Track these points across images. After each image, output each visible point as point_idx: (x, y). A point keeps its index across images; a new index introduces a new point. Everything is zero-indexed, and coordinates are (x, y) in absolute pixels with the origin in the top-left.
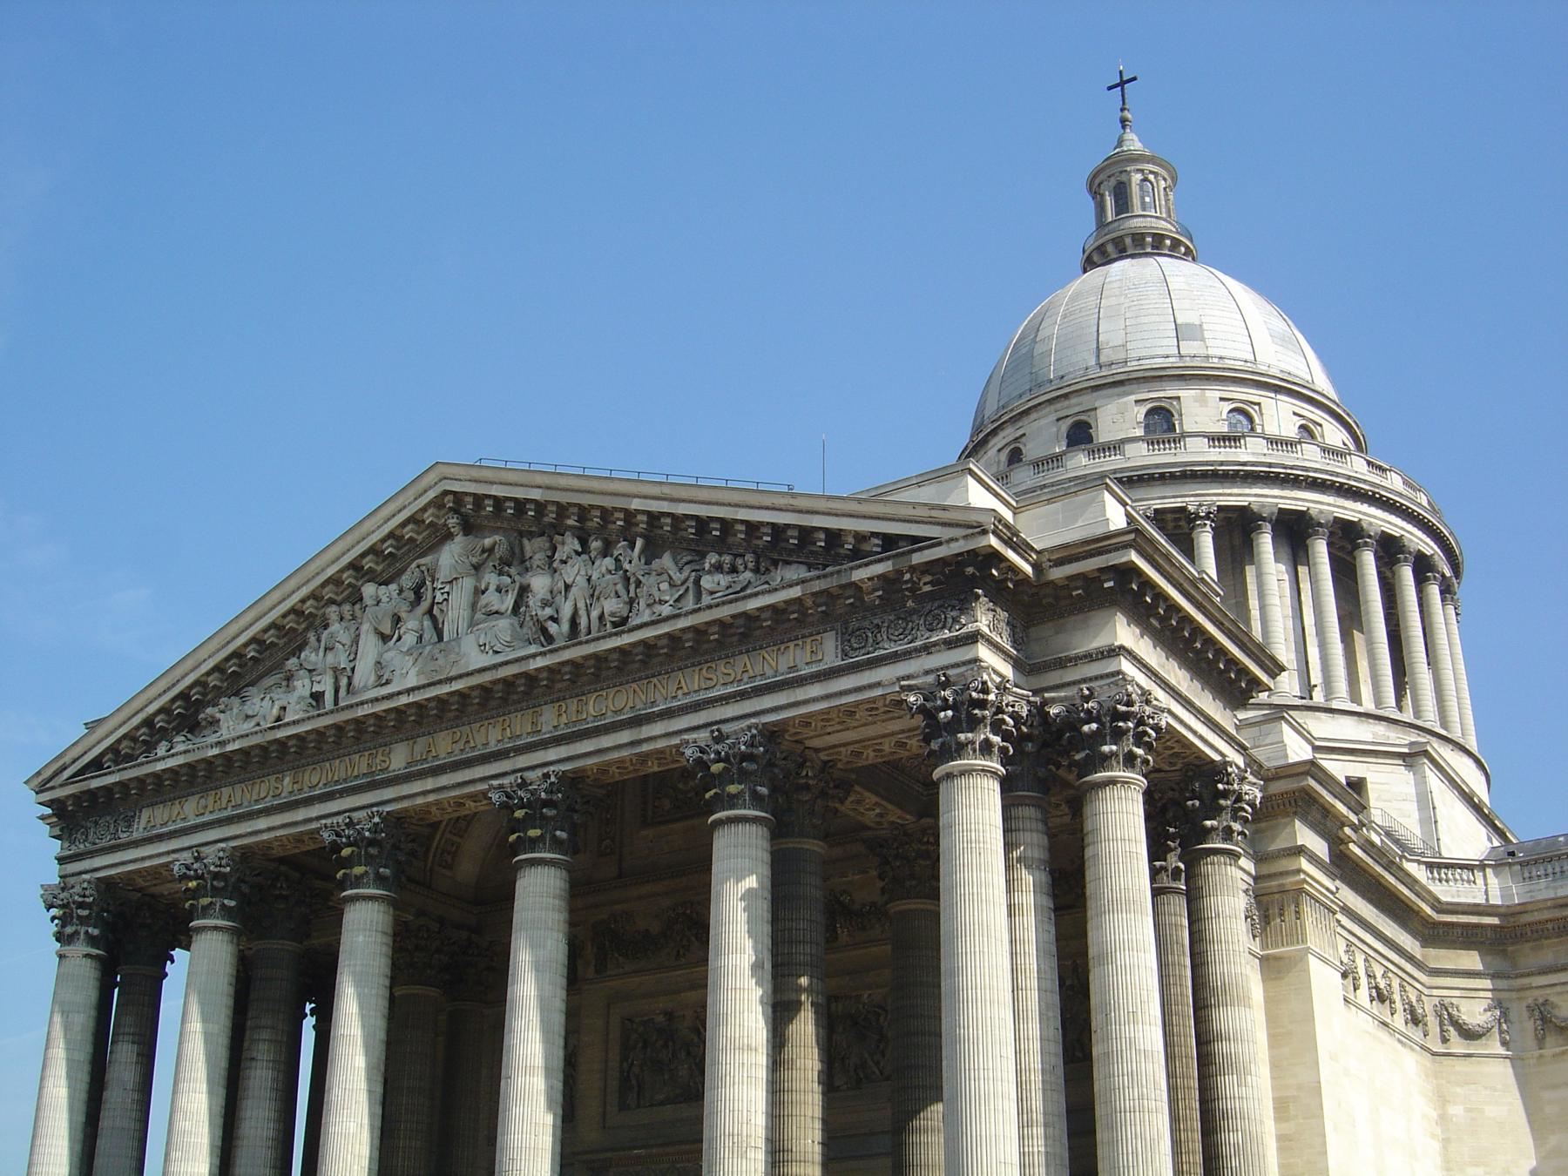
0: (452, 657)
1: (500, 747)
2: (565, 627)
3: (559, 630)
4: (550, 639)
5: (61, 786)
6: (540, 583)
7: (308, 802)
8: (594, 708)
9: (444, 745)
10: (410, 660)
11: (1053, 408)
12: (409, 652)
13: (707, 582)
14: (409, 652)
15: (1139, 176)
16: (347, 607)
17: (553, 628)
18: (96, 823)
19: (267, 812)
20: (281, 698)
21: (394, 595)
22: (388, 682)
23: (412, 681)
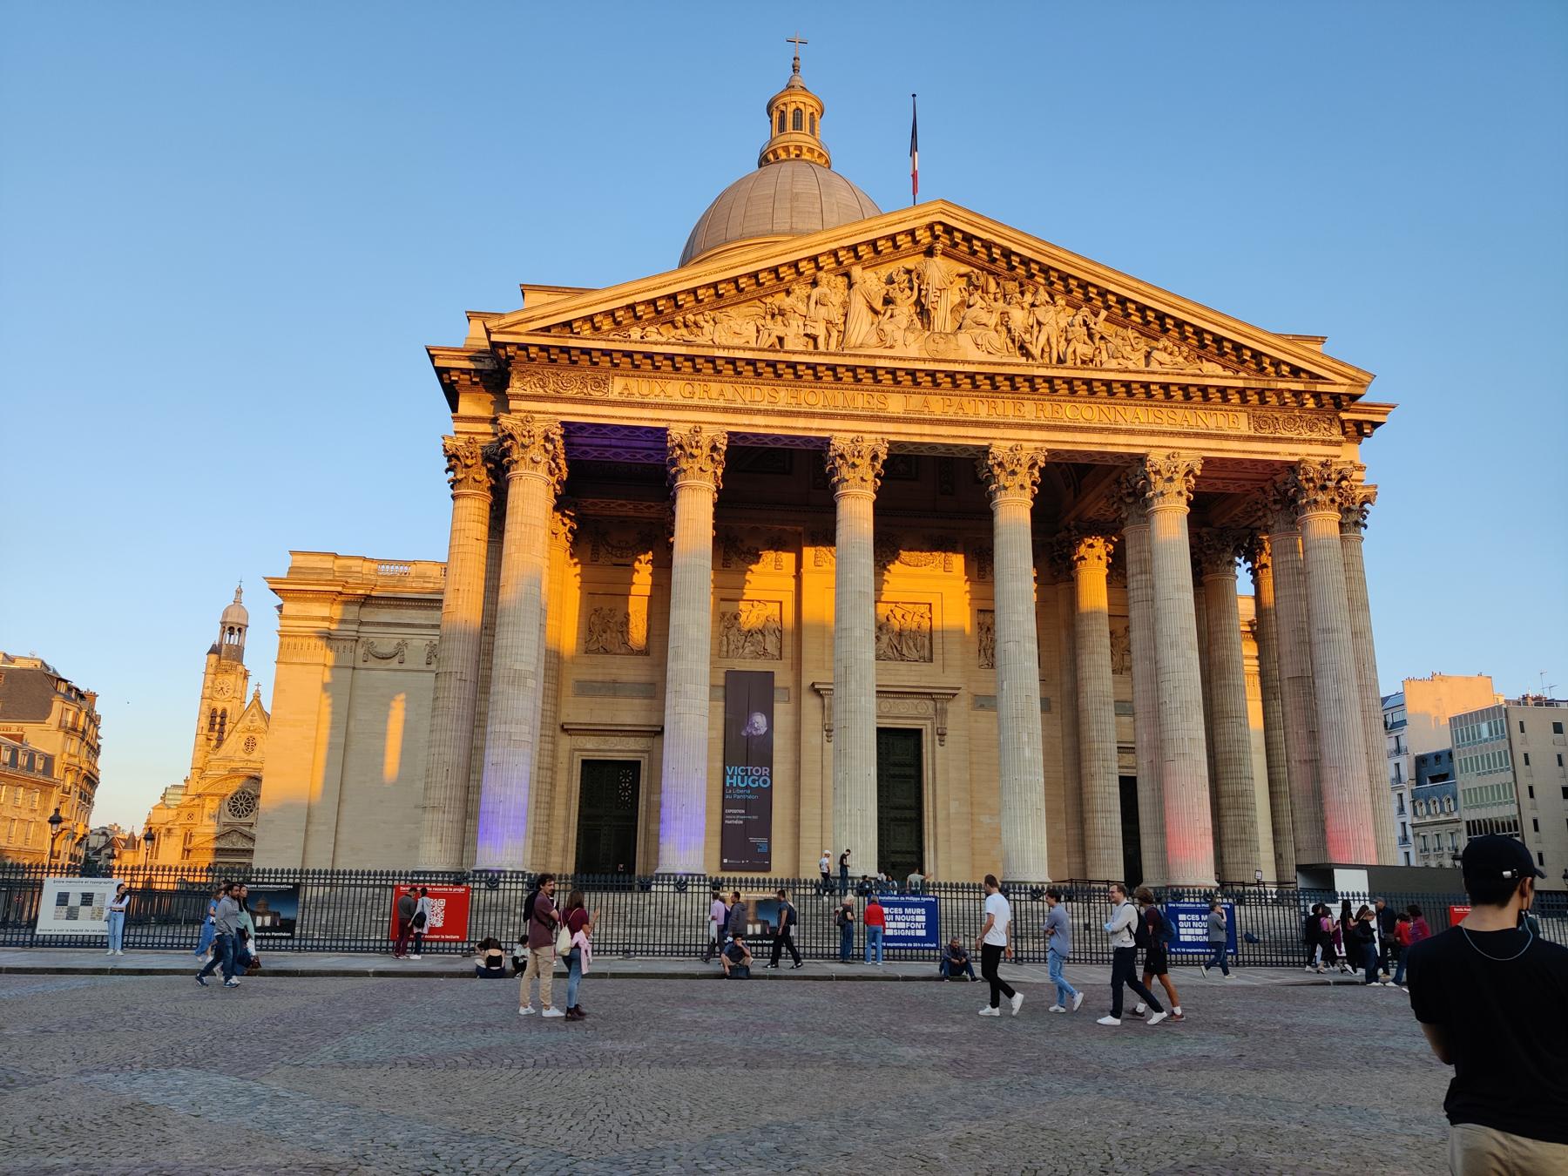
0: (952, 346)
3: (1036, 352)
4: (1027, 354)
5: (531, 333)
6: (1019, 318)
7: (812, 415)
8: (1070, 412)
9: (938, 405)
10: (911, 337)
13: (1155, 354)
15: (811, 110)
19: (766, 413)
23: (913, 352)
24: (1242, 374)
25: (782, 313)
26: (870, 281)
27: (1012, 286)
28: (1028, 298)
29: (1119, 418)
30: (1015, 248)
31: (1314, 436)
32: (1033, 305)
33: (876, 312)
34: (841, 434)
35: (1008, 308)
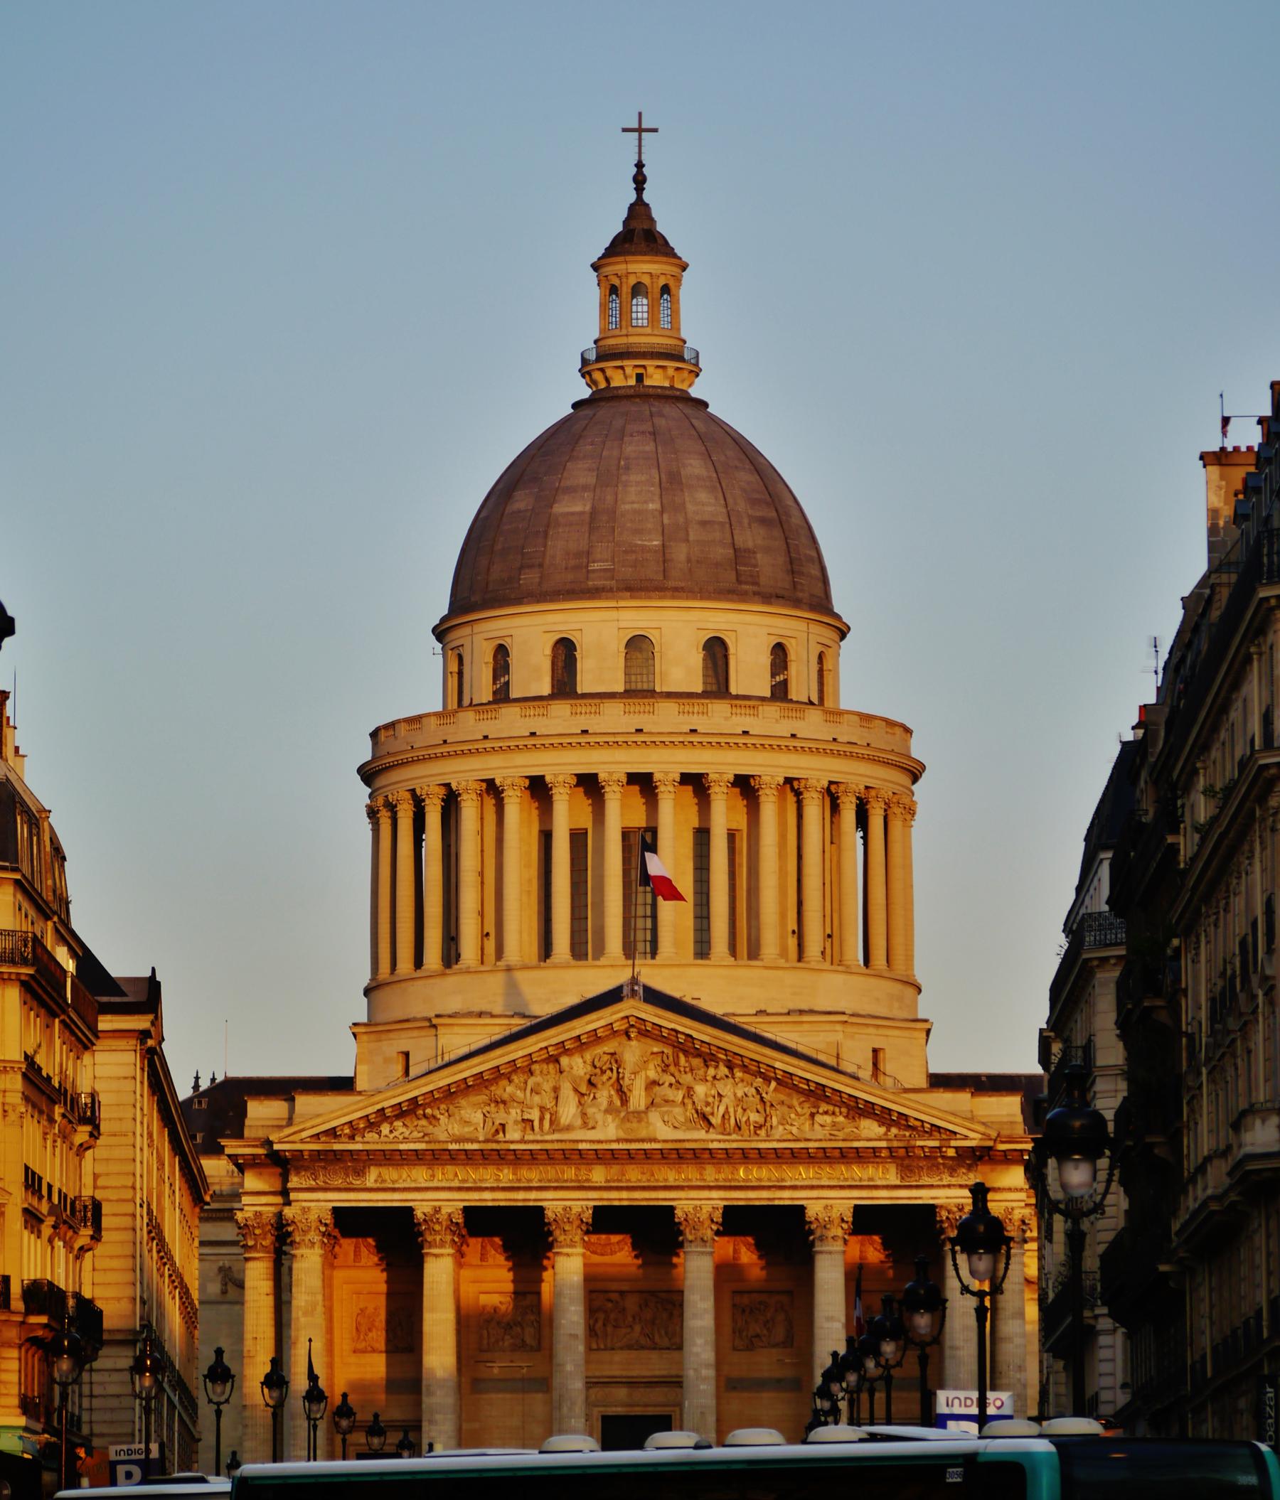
1: (677, 1184)
2: (719, 1120)
3: (716, 1120)
5: (302, 1141)
6: (700, 1090)
9: (634, 1174)
10: (610, 1118)
11: (613, 614)
12: (607, 1111)
13: (818, 1118)
14: (607, 1111)
16: (545, 1066)
17: (713, 1121)
18: (324, 1168)
19: (492, 1189)
20: (500, 1117)
21: (581, 1065)
22: (593, 1128)
24: (894, 1131)
25: (504, 1102)
26: (578, 1065)
27: (696, 1062)
28: (711, 1071)
29: (784, 1175)
30: (695, 1035)
31: (954, 1181)
32: (714, 1078)
33: (583, 1095)
34: (552, 1203)
35: (692, 1084)
